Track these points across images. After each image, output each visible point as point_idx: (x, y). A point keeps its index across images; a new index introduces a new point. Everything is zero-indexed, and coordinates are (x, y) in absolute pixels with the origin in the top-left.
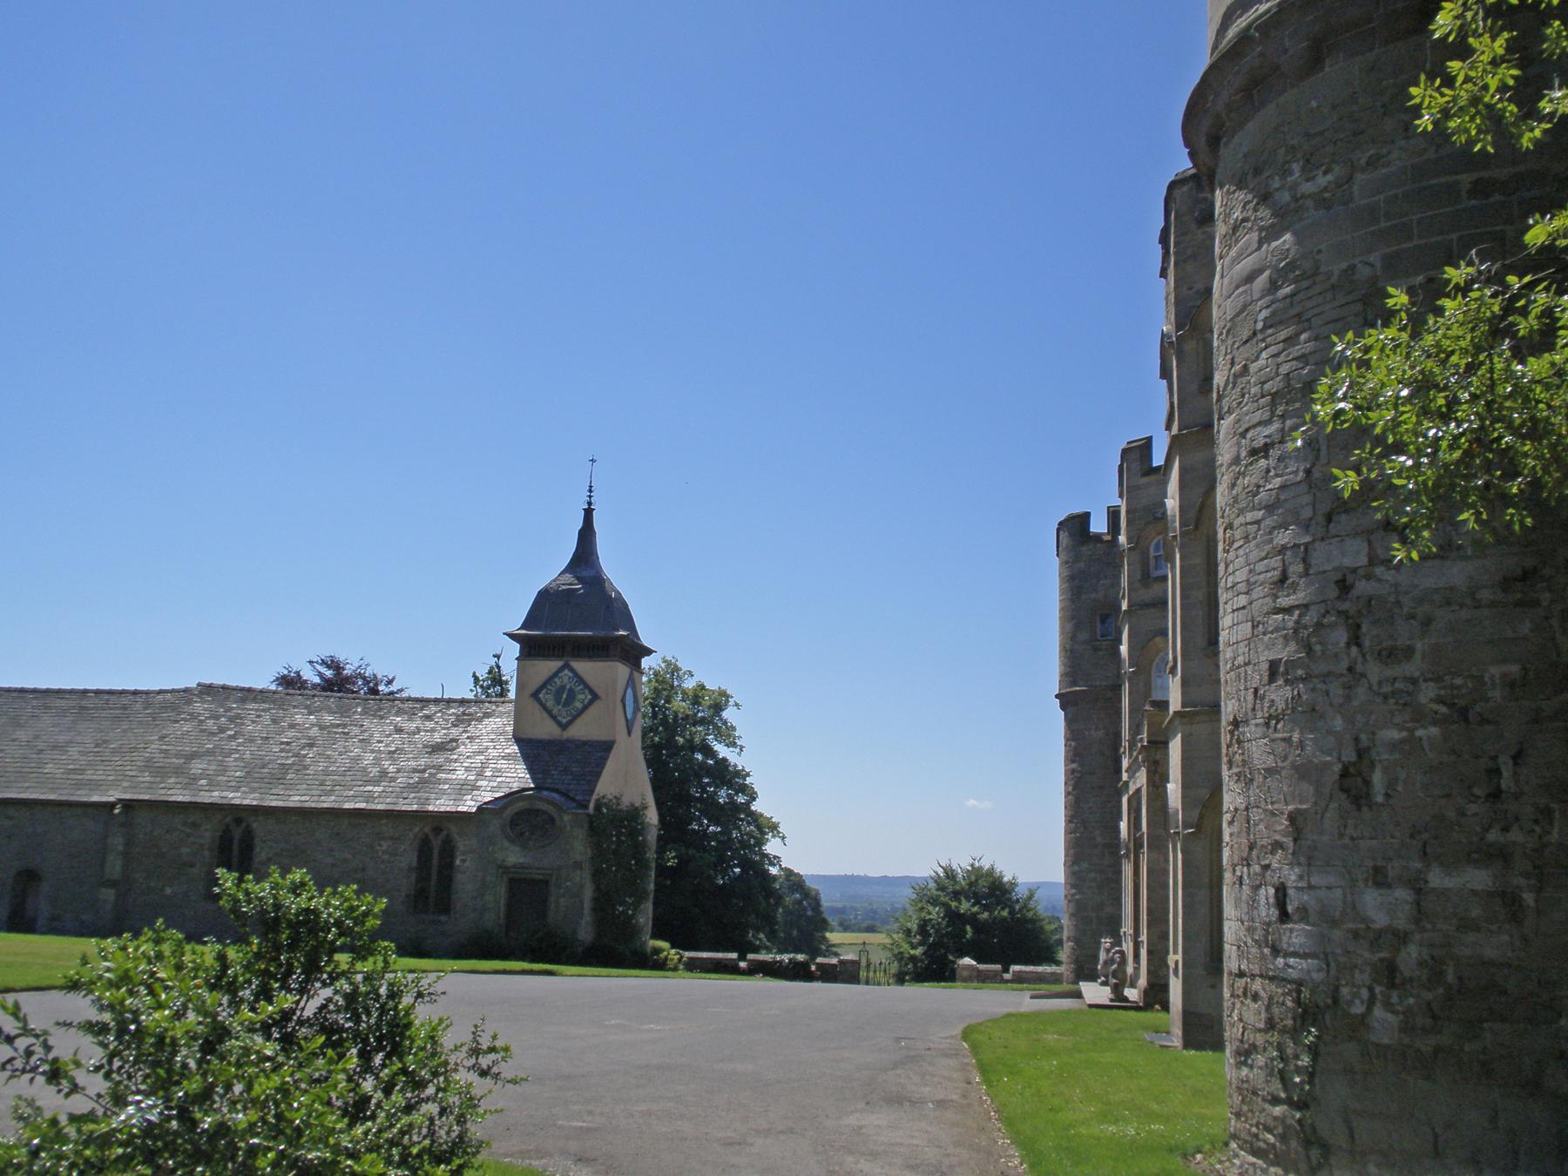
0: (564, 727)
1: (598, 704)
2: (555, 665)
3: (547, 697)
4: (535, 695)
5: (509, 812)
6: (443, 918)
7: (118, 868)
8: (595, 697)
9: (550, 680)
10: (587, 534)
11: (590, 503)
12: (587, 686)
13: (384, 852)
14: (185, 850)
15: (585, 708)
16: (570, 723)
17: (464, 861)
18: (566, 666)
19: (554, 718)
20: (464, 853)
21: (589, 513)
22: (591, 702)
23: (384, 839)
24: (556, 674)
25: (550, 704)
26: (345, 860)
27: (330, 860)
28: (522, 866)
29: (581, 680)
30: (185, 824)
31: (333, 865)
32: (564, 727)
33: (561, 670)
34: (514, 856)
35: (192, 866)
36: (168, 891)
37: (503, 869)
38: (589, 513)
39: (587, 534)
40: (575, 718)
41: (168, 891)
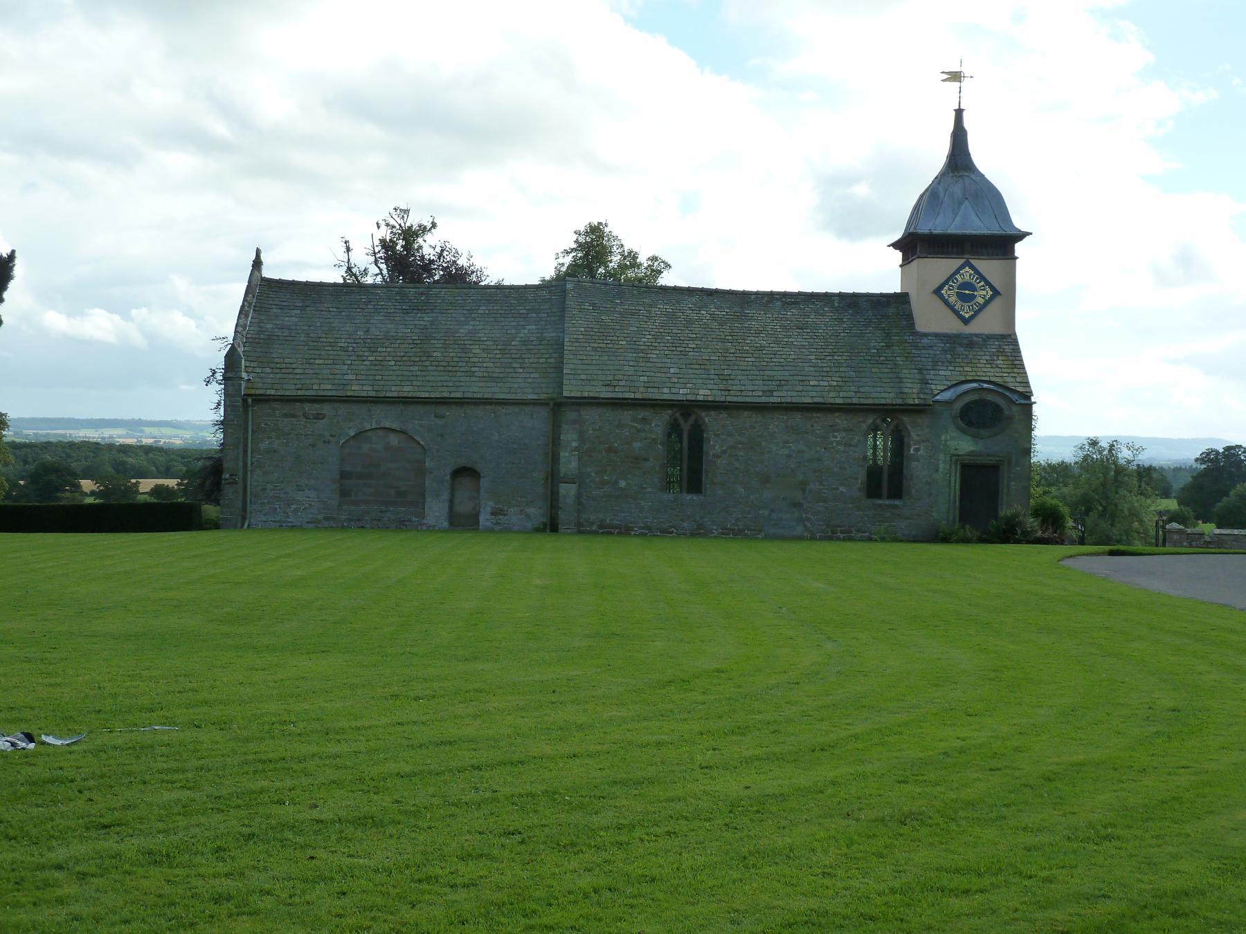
0: (966, 322)
1: (997, 302)
2: (956, 263)
3: (950, 294)
4: (937, 292)
5: (959, 405)
6: (897, 502)
7: (574, 465)
8: (996, 293)
9: (952, 277)
12: (988, 283)
13: (839, 443)
14: (637, 445)
15: (987, 302)
16: (972, 317)
17: (917, 450)
19: (956, 313)
20: (917, 443)
21: (959, 113)
22: (992, 298)
23: (837, 431)
24: (957, 272)
25: (953, 299)
26: (801, 452)
27: (787, 452)
28: (971, 454)
29: (982, 278)
30: (634, 420)
31: (789, 456)
32: (966, 322)
33: (962, 267)
34: (965, 445)
35: (646, 460)
36: (623, 484)
37: (955, 458)
38: (959, 113)
40: (976, 313)
41: (623, 484)
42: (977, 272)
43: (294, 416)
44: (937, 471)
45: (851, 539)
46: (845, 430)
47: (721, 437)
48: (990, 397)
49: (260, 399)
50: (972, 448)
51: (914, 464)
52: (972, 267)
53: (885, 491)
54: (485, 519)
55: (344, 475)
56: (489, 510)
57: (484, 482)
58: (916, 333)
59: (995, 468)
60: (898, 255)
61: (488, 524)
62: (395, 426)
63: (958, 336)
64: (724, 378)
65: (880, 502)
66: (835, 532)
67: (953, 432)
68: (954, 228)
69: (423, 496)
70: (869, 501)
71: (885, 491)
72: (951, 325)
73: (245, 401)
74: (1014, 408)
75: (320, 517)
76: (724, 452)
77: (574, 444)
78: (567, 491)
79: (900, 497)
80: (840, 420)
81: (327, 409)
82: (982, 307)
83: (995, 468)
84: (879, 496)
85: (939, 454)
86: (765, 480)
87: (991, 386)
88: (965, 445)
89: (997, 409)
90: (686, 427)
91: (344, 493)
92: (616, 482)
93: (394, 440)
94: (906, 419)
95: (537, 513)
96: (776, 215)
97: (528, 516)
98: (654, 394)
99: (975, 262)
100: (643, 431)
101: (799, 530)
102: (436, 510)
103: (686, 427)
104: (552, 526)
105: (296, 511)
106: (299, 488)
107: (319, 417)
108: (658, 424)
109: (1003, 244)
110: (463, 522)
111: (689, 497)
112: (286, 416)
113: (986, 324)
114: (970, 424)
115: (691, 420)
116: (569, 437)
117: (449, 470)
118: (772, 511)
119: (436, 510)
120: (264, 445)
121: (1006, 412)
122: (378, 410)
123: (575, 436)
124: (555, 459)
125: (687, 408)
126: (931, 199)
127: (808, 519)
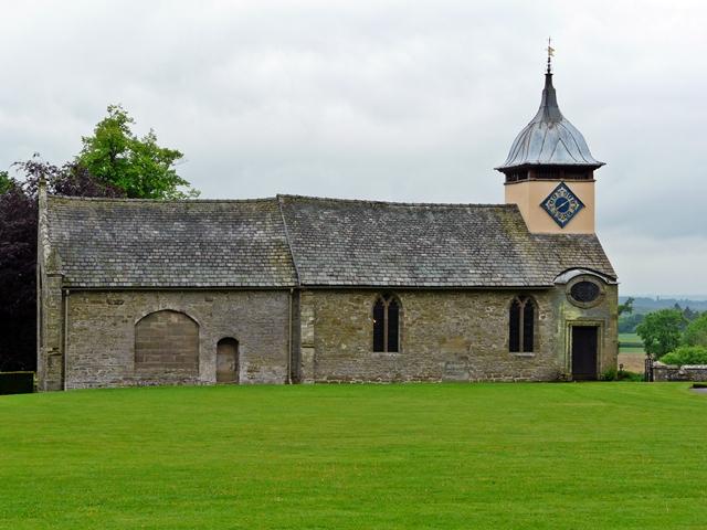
1: (583, 211)
4: (543, 205)
5: (571, 285)
6: (531, 354)
7: (311, 334)
8: (582, 205)
10: (549, 93)
11: (549, 70)
13: (491, 314)
14: (354, 318)
15: (576, 212)
16: (566, 223)
17: (543, 317)
18: (563, 185)
19: (556, 220)
21: (549, 76)
22: (578, 210)
24: (555, 191)
25: (553, 210)
27: (456, 321)
28: (578, 319)
31: (458, 324)
34: (574, 314)
35: (360, 329)
36: (344, 347)
38: (549, 76)
39: (549, 93)
41: (344, 347)
42: (569, 191)
43: (101, 303)
44: (557, 331)
45: (497, 381)
46: (495, 304)
47: (411, 313)
48: (590, 280)
49: (76, 291)
50: (579, 315)
51: (541, 327)
52: (567, 188)
53: (522, 346)
54: (243, 375)
55: (136, 346)
56: (246, 368)
57: (242, 349)
58: (529, 234)
59: (594, 329)
60: (503, 176)
61: (246, 379)
62: (176, 308)
63: (556, 237)
64: (412, 269)
65: (519, 354)
66: (490, 378)
67: (566, 304)
68: (554, 160)
69: (198, 360)
70: (512, 354)
71: (522, 346)
72: (552, 229)
73: (64, 292)
74: (606, 287)
75: (121, 378)
76: (414, 322)
77: (311, 319)
78: (307, 354)
79: (531, 351)
80: (493, 299)
81: (125, 297)
82: (572, 216)
83: (594, 329)
84: (518, 351)
85: (557, 323)
86: (443, 341)
87: (588, 272)
88: (574, 314)
89: (596, 288)
90: (386, 304)
91: (137, 359)
92: (340, 345)
93: (174, 319)
94: (536, 296)
95: (281, 370)
96: (451, 155)
97: (274, 372)
98: (364, 281)
99: (567, 184)
100: (357, 308)
101: (466, 376)
102: (207, 371)
103: (386, 304)
104: (295, 377)
105: (102, 374)
106: (105, 357)
107: (117, 303)
108: (368, 304)
109: (585, 172)
110: (228, 378)
111: (390, 354)
112: (94, 302)
113: (574, 228)
114: (578, 299)
115: (390, 300)
116: (307, 314)
117: (216, 340)
118: (448, 363)
119: (207, 371)
120: (76, 325)
121: (602, 290)
122: (163, 298)
123: (312, 313)
124: (296, 330)
125: (390, 293)
126: (523, 140)
127: (472, 368)
